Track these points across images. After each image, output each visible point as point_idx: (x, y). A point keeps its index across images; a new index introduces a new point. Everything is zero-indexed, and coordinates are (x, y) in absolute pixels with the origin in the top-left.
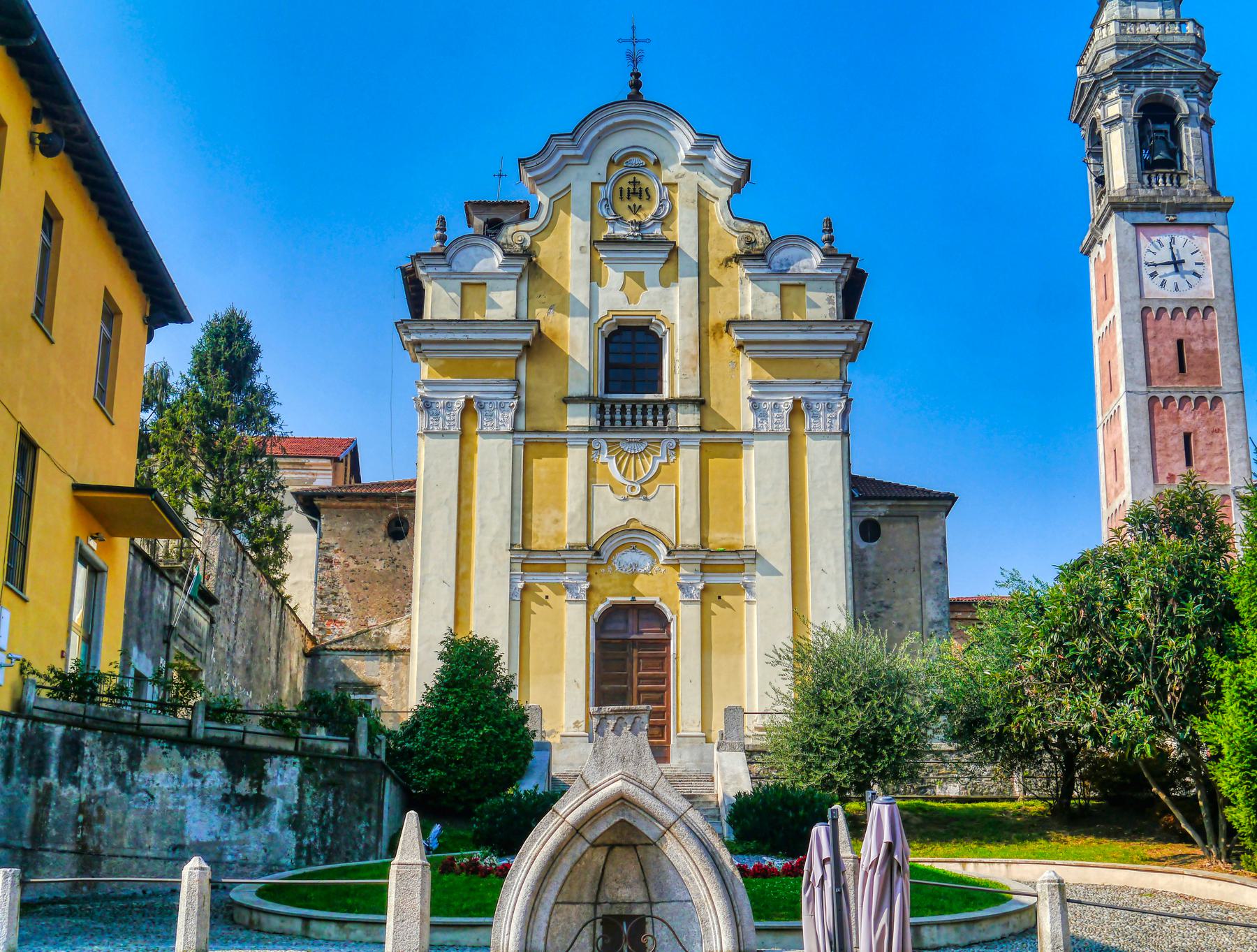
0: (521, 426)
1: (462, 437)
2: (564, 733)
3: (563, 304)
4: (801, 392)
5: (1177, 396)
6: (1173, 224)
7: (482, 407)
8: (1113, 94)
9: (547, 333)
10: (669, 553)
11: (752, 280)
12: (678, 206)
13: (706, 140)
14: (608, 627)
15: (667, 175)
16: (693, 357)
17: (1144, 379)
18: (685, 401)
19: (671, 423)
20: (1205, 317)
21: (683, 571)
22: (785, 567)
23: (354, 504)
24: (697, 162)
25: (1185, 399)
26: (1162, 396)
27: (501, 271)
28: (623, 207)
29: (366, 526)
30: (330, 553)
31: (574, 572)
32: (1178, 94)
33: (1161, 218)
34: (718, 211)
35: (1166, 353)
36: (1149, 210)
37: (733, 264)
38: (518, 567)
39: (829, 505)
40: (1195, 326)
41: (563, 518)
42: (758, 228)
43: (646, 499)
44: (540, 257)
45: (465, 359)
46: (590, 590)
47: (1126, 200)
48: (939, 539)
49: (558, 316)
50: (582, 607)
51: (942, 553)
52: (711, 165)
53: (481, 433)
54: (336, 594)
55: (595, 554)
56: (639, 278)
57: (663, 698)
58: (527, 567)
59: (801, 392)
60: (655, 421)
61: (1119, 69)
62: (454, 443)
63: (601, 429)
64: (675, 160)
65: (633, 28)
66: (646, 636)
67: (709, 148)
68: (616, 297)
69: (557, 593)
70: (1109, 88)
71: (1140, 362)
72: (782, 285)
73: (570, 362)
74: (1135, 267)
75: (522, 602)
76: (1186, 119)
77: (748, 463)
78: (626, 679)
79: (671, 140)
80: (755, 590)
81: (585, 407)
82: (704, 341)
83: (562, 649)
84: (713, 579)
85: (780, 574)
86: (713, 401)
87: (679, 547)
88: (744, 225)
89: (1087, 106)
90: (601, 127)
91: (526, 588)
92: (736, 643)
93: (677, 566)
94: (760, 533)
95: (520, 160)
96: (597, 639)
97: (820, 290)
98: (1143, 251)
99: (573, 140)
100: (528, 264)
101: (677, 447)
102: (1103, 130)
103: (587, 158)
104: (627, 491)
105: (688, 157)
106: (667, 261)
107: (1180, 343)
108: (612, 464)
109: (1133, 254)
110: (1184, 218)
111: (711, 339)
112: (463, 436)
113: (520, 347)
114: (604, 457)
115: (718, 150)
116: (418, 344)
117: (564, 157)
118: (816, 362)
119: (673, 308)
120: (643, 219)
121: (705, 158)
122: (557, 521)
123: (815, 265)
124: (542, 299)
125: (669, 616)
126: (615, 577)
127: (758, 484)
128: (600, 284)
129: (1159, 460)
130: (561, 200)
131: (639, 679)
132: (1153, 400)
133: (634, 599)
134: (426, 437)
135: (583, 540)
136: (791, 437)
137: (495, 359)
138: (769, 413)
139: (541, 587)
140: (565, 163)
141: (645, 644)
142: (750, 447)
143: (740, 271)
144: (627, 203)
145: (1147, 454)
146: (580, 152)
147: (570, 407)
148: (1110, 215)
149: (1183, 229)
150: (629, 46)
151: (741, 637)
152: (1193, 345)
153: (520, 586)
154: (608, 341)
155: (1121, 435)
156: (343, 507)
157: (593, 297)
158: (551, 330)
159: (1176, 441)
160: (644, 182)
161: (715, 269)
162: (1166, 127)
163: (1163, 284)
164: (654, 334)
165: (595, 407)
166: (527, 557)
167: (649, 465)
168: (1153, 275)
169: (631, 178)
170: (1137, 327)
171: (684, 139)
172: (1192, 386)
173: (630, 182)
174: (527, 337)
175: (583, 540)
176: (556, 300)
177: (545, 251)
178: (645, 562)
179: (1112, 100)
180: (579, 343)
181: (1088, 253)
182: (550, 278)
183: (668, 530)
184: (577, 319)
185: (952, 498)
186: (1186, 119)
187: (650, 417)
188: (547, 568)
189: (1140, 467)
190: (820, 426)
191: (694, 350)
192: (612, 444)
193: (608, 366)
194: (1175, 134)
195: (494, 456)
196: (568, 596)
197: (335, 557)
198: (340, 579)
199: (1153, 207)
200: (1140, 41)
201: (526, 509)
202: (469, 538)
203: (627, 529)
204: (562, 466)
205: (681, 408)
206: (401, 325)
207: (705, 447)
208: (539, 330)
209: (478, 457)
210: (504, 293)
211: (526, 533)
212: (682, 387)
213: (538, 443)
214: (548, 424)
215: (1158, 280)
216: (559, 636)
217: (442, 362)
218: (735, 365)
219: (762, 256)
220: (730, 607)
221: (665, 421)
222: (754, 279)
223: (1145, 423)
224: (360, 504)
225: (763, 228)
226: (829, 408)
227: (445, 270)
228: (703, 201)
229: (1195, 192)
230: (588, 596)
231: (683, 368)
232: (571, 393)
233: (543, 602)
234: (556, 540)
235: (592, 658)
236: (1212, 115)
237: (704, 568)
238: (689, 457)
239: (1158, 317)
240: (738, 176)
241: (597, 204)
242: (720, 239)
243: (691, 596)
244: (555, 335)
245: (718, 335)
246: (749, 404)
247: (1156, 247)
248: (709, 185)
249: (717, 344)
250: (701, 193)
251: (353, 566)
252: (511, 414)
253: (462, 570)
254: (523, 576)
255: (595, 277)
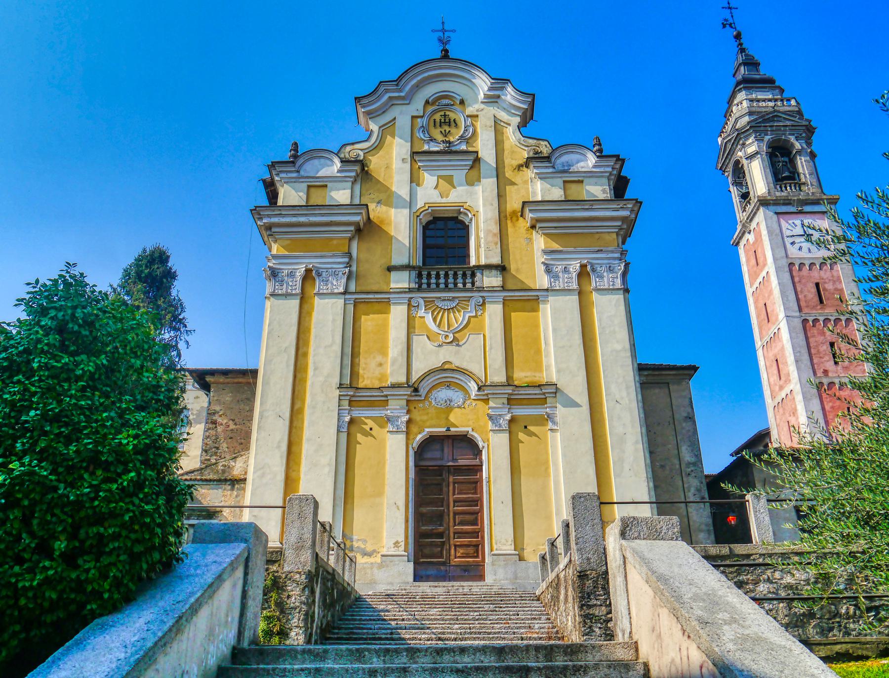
0: (352, 287)
1: (302, 299)
2: (384, 551)
3: (388, 198)
4: (585, 258)
5: (821, 319)
6: (801, 212)
7: (319, 275)
8: (750, 141)
9: (375, 221)
10: (479, 389)
11: (540, 178)
12: (479, 130)
13: (499, 82)
14: (428, 455)
15: (470, 110)
16: (495, 235)
17: (797, 309)
18: (489, 267)
19: (477, 284)
20: (831, 269)
21: (491, 404)
22: (583, 399)
23: (236, 380)
24: (493, 99)
25: (827, 321)
26: (811, 319)
27: (339, 175)
28: (437, 134)
29: (244, 396)
30: (216, 417)
31: (396, 407)
32: (792, 139)
33: (793, 209)
34: (511, 135)
35: (809, 291)
36: (784, 204)
37: (525, 169)
38: (347, 403)
39: (618, 347)
40: (826, 274)
41: (386, 362)
42: (542, 143)
43: (458, 345)
44: (371, 167)
45: (308, 239)
46: (409, 422)
47: (769, 198)
48: (687, 400)
49: (384, 208)
50: (402, 437)
51: (690, 410)
52: (505, 101)
53: (318, 294)
54: (218, 448)
55: (414, 391)
56: (449, 180)
57: (476, 519)
58: (353, 403)
59: (585, 258)
60: (464, 284)
61: (753, 124)
62: (295, 303)
63: (419, 289)
64: (476, 101)
65: (443, 23)
66: (462, 462)
67: (502, 89)
68: (431, 193)
69: (382, 426)
70: (747, 138)
71: (792, 297)
72: (565, 182)
73: (393, 241)
74: (779, 240)
75: (349, 434)
76: (799, 152)
77: (545, 316)
78: (441, 502)
79: (472, 86)
80: (558, 419)
81: (405, 274)
82: (503, 224)
83: (384, 474)
84: (520, 411)
85: (577, 405)
86: (513, 267)
87: (488, 383)
88: (531, 141)
89: (732, 152)
90: (419, 78)
91: (352, 422)
92: (542, 467)
93: (486, 401)
94: (558, 371)
95: (356, 98)
96: (416, 466)
97: (596, 184)
98: (784, 229)
99: (397, 85)
100: (361, 172)
101: (484, 303)
102: (745, 162)
103: (408, 99)
104: (441, 339)
105: (486, 96)
106: (472, 167)
107: (817, 285)
108: (429, 318)
109: (778, 231)
110: (807, 208)
111: (509, 222)
112: (304, 299)
113: (352, 228)
114: (421, 312)
115: (509, 89)
116: (269, 227)
117: (390, 98)
118: (597, 236)
119: (478, 202)
120: (452, 139)
121: (499, 97)
122: (380, 365)
123: (591, 165)
124: (372, 196)
125: (481, 444)
126: (432, 411)
127: (554, 330)
128: (418, 185)
129: (815, 361)
130: (388, 129)
131: (455, 502)
132: (805, 322)
133: (448, 430)
134: (272, 299)
135: (403, 379)
136: (580, 293)
137: (332, 239)
138: (560, 275)
139: (366, 421)
140: (391, 103)
141: (459, 470)
142: (545, 302)
143: (530, 173)
144: (439, 129)
145: (806, 357)
146: (402, 94)
147: (393, 274)
148: (758, 209)
149: (808, 216)
150: (441, 34)
151: (547, 462)
152: (826, 286)
153: (347, 419)
154: (426, 228)
155: (783, 349)
156: (228, 383)
157: (412, 194)
158: (379, 218)
159: (825, 347)
160: (452, 116)
161: (510, 172)
162: (786, 159)
163: (800, 249)
164: (462, 223)
165: (414, 274)
166: (353, 392)
167: (459, 318)
168: (793, 243)
169: (442, 113)
170: (787, 276)
171: (482, 83)
172: (830, 312)
173: (442, 113)
174: (357, 219)
175: (403, 379)
176: (383, 196)
177: (375, 163)
178: (457, 397)
179: (750, 144)
180: (401, 228)
181: (738, 244)
182: (378, 182)
183: (477, 369)
184: (399, 210)
185: (694, 369)
186: (799, 152)
187: (460, 280)
188: (371, 404)
189: (803, 366)
190: (605, 284)
191: (496, 229)
192: (428, 303)
193: (425, 247)
194: (792, 162)
195: (328, 313)
196: (390, 427)
197: (219, 420)
198: (222, 436)
199: (787, 202)
200: (764, 110)
201: (355, 355)
202: (304, 380)
203: (441, 370)
204: (387, 320)
205: (486, 272)
206: (256, 212)
207: (506, 302)
208: (369, 218)
209: (315, 315)
210: (341, 192)
211: (354, 374)
212: (486, 257)
213: (366, 302)
214: (375, 288)
215: (797, 246)
216: (381, 464)
217: (288, 242)
218: (530, 240)
219: (548, 158)
220: (536, 435)
221: (473, 284)
222: (542, 177)
223: (802, 336)
224: (240, 380)
225: (546, 143)
226: (610, 269)
227: (294, 175)
228: (499, 127)
229: (813, 193)
230: (407, 427)
231: (487, 243)
232: (393, 263)
233: (367, 434)
234: (380, 380)
235: (411, 483)
236: (815, 151)
237: (510, 401)
238: (494, 312)
239: (800, 269)
240: (525, 107)
241: (416, 131)
242: (513, 152)
243: (500, 426)
244: (382, 221)
245: (514, 219)
246: (543, 268)
247: (793, 226)
248: (503, 116)
249: (514, 226)
250: (496, 121)
251: (232, 427)
252: (344, 280)
253: (297, 407)
254: (350, 410)
255: (414, 180)
